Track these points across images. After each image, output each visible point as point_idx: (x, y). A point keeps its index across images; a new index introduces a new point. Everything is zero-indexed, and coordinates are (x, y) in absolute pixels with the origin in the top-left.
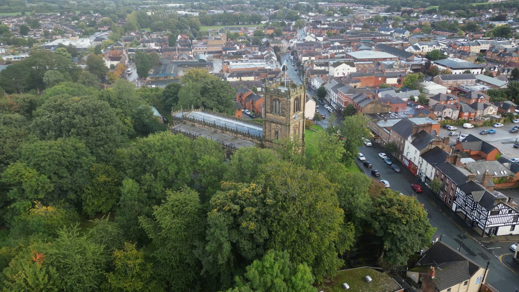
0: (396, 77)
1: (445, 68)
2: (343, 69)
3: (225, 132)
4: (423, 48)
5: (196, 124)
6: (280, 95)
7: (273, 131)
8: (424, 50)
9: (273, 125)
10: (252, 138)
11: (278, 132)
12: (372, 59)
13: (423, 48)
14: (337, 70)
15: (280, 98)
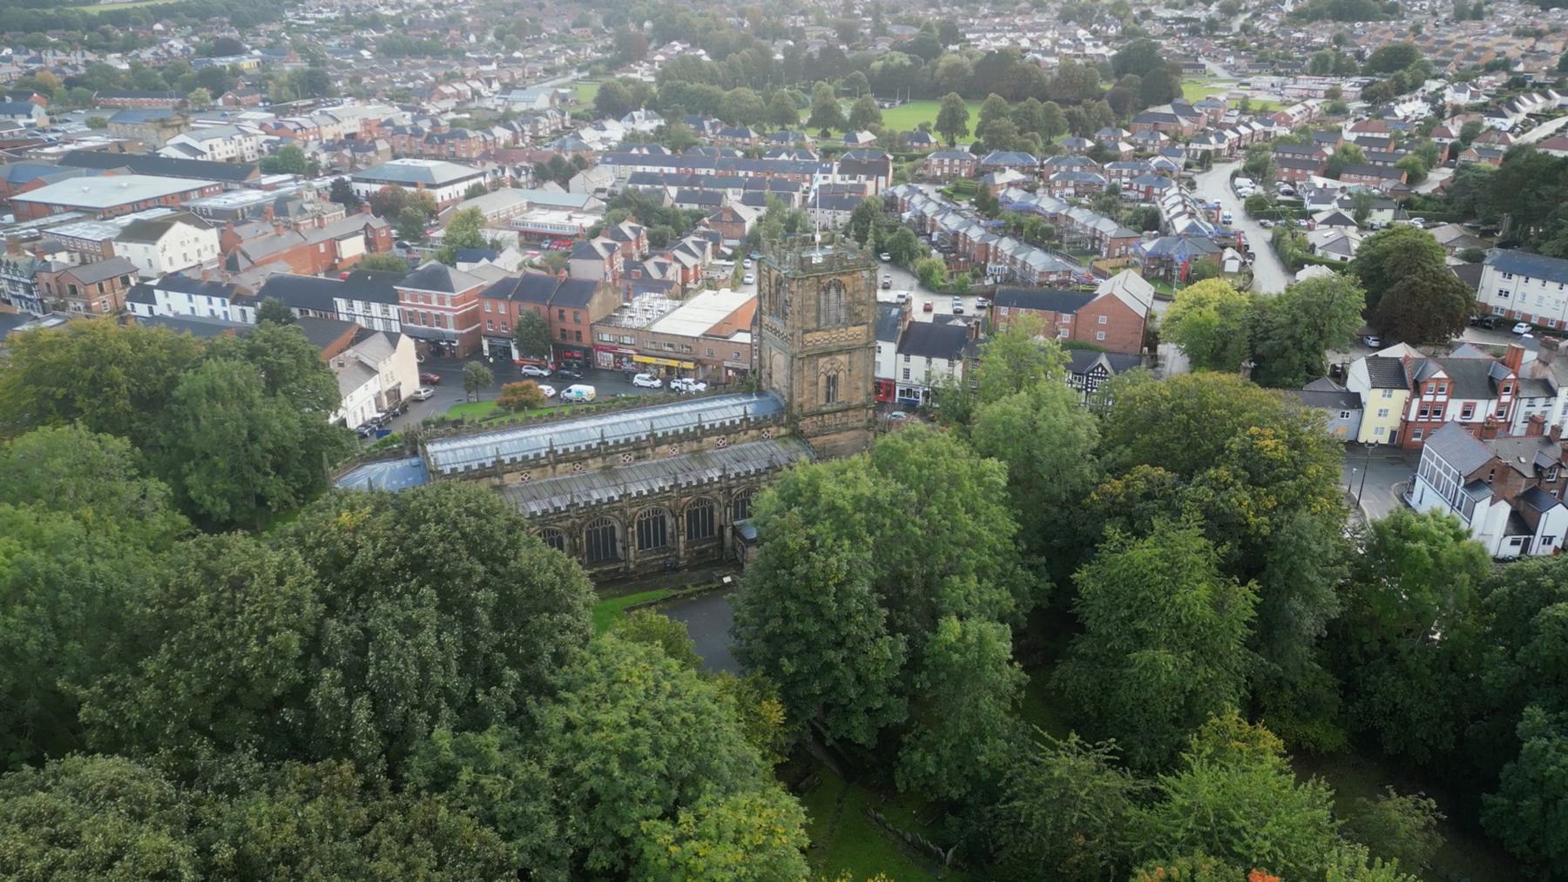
0: (356, 233)
1: (413, 189)
2: (182, 243)
3: (649, 451)
4: (211, 148)
5: (507, 477)
6: (847, 267)
7: (822, 380)
8: (216, 152)
9: (822, 361)
10: (760, 429)
11: (835, 377)
12: (146, 201)
13: (211, 148)
14: (164, 249)
15: (844, 279)
